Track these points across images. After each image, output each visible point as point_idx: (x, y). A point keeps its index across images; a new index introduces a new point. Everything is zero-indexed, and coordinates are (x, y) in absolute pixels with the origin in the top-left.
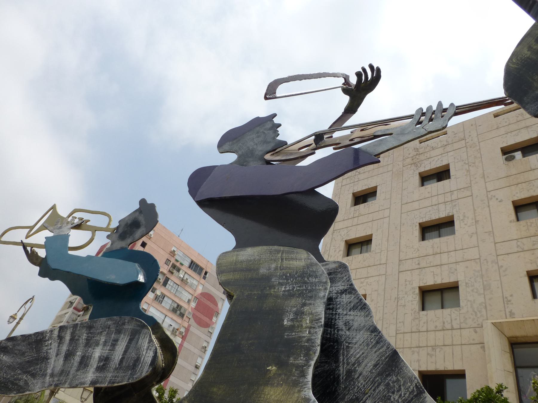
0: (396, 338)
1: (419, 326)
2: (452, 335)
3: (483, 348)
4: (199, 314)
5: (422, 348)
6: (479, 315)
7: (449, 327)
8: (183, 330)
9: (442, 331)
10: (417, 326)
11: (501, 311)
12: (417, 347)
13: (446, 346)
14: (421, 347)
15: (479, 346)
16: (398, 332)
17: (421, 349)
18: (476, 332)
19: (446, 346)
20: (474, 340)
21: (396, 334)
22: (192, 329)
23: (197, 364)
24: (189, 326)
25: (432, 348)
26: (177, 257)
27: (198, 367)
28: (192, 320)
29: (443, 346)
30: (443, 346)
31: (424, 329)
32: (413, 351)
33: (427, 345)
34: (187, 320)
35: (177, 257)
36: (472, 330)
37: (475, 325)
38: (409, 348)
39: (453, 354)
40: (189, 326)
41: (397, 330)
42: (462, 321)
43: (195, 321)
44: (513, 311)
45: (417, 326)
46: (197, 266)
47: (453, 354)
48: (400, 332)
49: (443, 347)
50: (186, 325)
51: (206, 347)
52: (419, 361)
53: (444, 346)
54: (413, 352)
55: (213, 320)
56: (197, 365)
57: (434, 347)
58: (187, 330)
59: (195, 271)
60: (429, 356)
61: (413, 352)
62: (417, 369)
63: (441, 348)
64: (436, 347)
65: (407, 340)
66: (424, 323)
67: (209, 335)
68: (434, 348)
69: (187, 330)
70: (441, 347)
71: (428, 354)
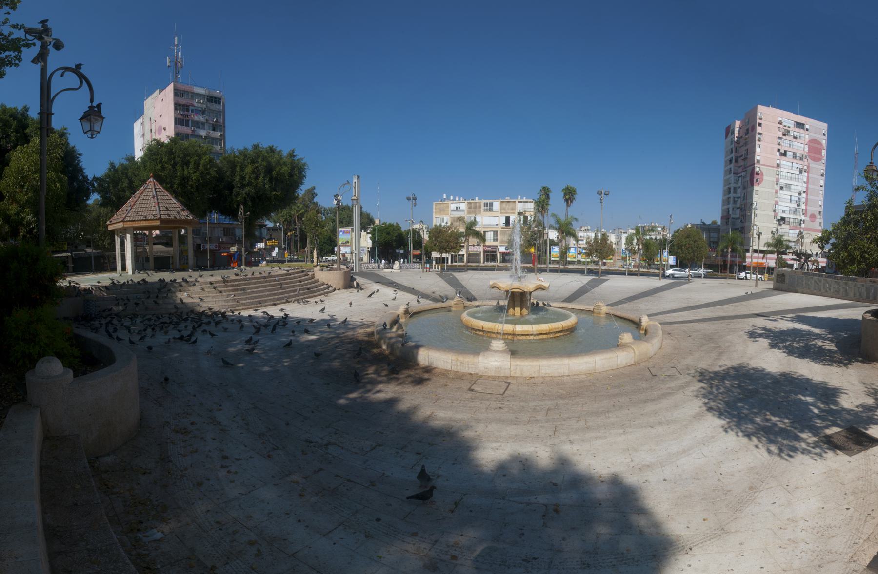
4: (812, 155)
8: (806, 167)
22: (811, 165)
24: (809, 164)
26: (784, 124)
34: (806, 160)
35: (784, 124)
40: (809, 164)
46: (800, 124)
50: (806, 164)
58: (808, 167)
69: (808, 167)
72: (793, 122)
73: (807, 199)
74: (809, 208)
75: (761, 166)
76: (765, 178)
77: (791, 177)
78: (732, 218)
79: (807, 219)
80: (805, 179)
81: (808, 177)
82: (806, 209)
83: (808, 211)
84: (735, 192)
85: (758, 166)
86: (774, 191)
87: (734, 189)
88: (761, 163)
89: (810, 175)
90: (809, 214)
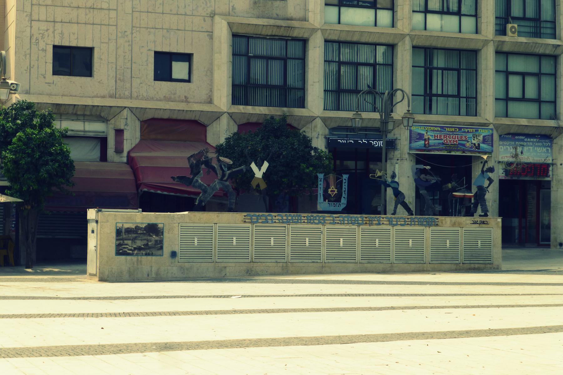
0: (132, 16)
1: (155, 7)
2: (185, 20)
3: (211, 37)
5: (159, 30)
6: (208, 5)
7: (182, 11)
9: (177, 16)
10: (153, 6)
11: (226, 4)
12: (153, 28)
13: (179, 30)
14: (157, 28)
15: (206, 34)
16: (134, 10)
17: (157, 30)
18: (205, 21)
19: (179, 30)
20: (202, 28)
21: (133, 11)
25: (168, 31)
29: (176, 30)
30: (176, 30)
31: (160, 10)
32: (149, 32)
33: (162, 27)
36: (201, 18)
37: (205, 14)
38: (145, 28)
39: (185, 39)
41: (133, 8)
42: (194, 8)
44: (234, 6)
45: (153, 6)
47: (185, 39)
48: (137, 10)
49: (177, 31)
52: (155, 42)
53: (177, 30)
54: (150, 33)
57: (169, 30)
60: (164, 38)
61: (150, 33)
62: (154, 49)
63: (175, 32)
64: (171, 30)
65: (143, 20)
66: (160, 4)
68: (168, 30)
70: (175, 31)
71: (163, 36)
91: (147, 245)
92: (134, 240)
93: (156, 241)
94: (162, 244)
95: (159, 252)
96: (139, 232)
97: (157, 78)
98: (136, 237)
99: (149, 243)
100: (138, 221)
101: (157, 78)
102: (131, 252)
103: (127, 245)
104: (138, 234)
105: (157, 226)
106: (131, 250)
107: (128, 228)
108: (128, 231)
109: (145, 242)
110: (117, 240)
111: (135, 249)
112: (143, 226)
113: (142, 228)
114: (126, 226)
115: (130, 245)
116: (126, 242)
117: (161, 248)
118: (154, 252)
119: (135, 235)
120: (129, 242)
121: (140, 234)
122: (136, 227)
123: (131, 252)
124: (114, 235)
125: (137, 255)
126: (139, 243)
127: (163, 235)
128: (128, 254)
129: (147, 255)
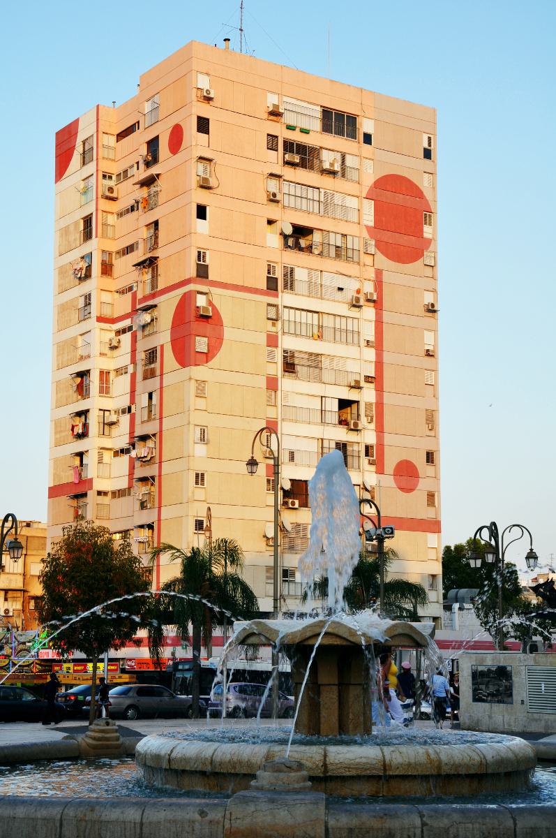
4: (387, 237)
22: (386, 277)
23: (427, 347)
24: (379, 273)
26: (289, 119)
27: (431, 353)
28: (380, 257)
34: (368, 260)
35: (289, 119)
40: (379, 273)
43: (387, 256)
46: (340, 115)
51: (433, 305)
55: (425, 235)
56: (428, 350)
58: (379, 284)
59: (340, 132)
67: (428, 271)
69: (379, 284)
72: (319, 109)
73: (380, 405)
74: (388, 439)
75: (214, 290)
76: (228, 333)
77: (320, 327)
78: (99, 493)
79: (389, 481)
80: (369, 333)
81: (379, 323)
82: (380, 445)
83: (386, 449)
84: (105, 390)
85: (204, 289)
86: (263, 383)
87: (101, 379)
88: (212, 275)
89: (387, 317)
90: (390, 464)
91: (498, 691)
92: (487, 685)
93: (506, 686)
94: (512, 690)
95: (510, 699)
96: (491, 675)
97: (428, 505)
98: (489, 682)
99: (501, 689)
100: (489, 663)
101: (428, 505)
102: (485, 698)
103: (481, 690)
104: (489, 677)
105: (506, 668)
106: (485, 696)
107: (482, 671)
108: (482, 674)
109: (496, 687)
110: (473, 684)
111: (489, 694)
112: (494, 669)
113: (493, 671)
114: (480, 668)
115: (484, 689)
116: (480, 686)
117: (511, 695)
118: (505, 699)
119: (487, 679)
120: (483, 687)
121: (493, 677)
122: (489, 670)
123: (485, 698)
124: (470, 678)
125: (490, 702)
126: (492, 689)
127: (511, 679)
128: (483, 701)
129: (499, 702)
